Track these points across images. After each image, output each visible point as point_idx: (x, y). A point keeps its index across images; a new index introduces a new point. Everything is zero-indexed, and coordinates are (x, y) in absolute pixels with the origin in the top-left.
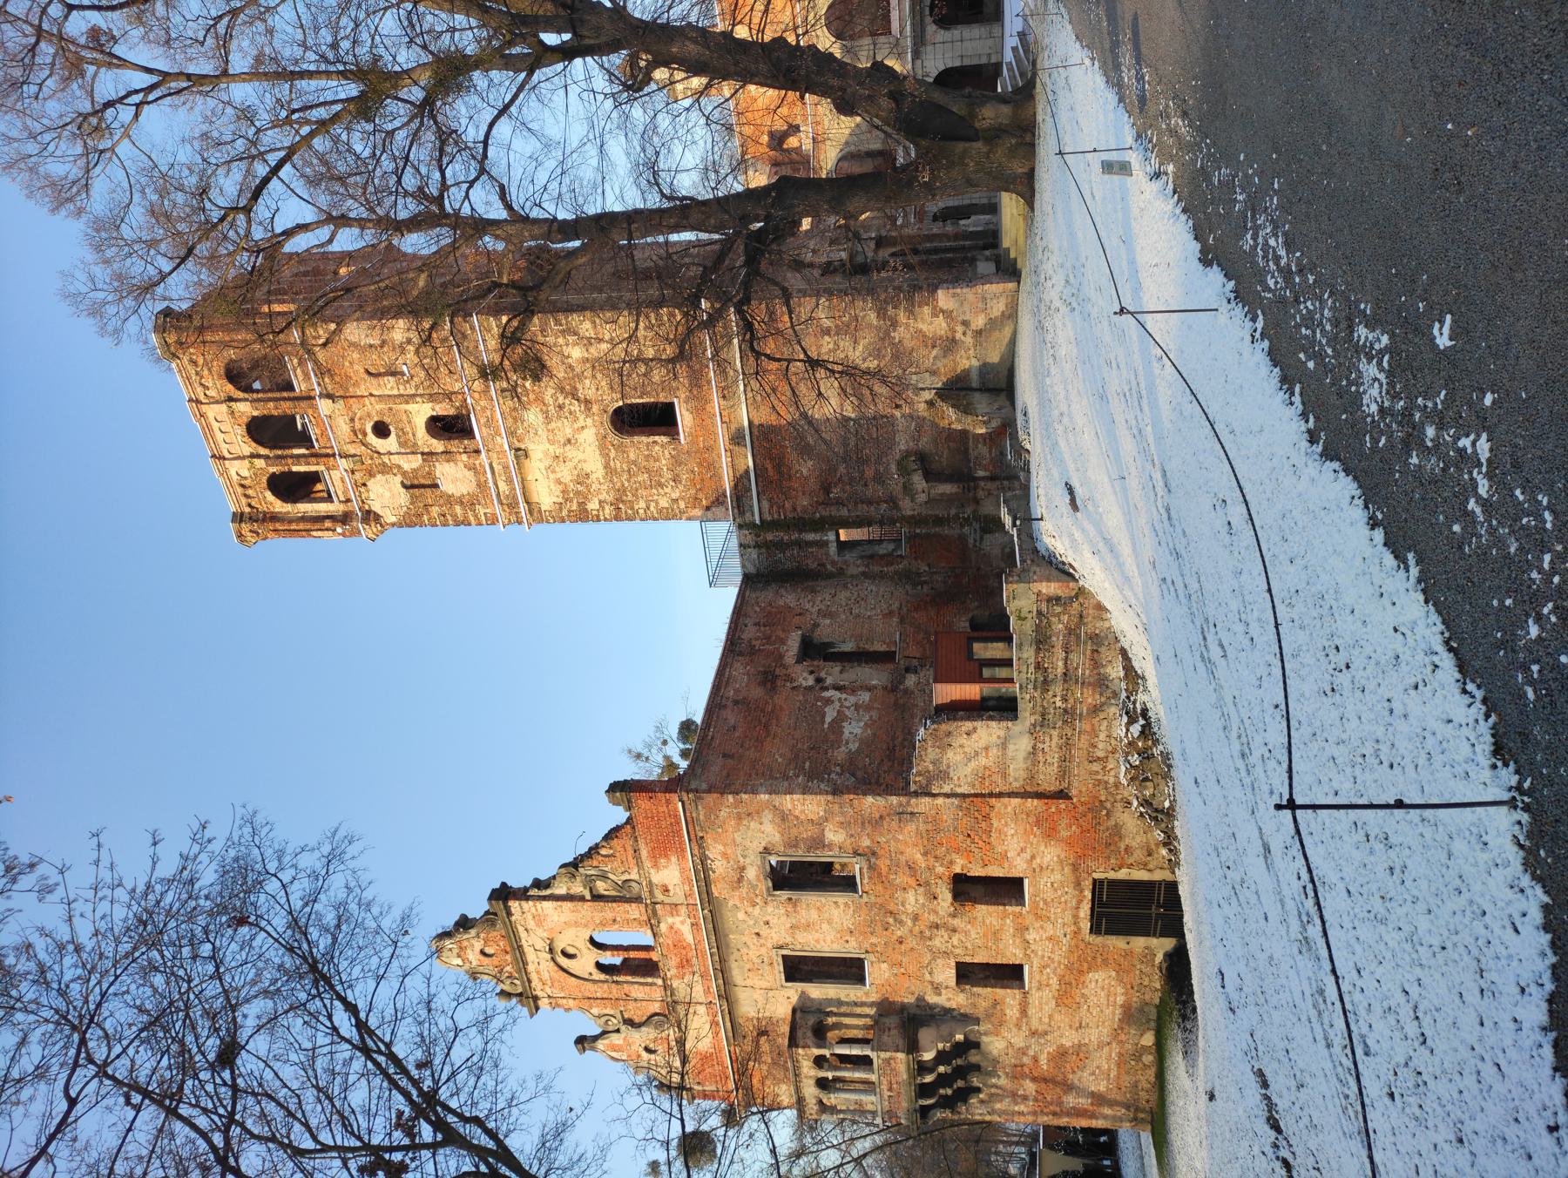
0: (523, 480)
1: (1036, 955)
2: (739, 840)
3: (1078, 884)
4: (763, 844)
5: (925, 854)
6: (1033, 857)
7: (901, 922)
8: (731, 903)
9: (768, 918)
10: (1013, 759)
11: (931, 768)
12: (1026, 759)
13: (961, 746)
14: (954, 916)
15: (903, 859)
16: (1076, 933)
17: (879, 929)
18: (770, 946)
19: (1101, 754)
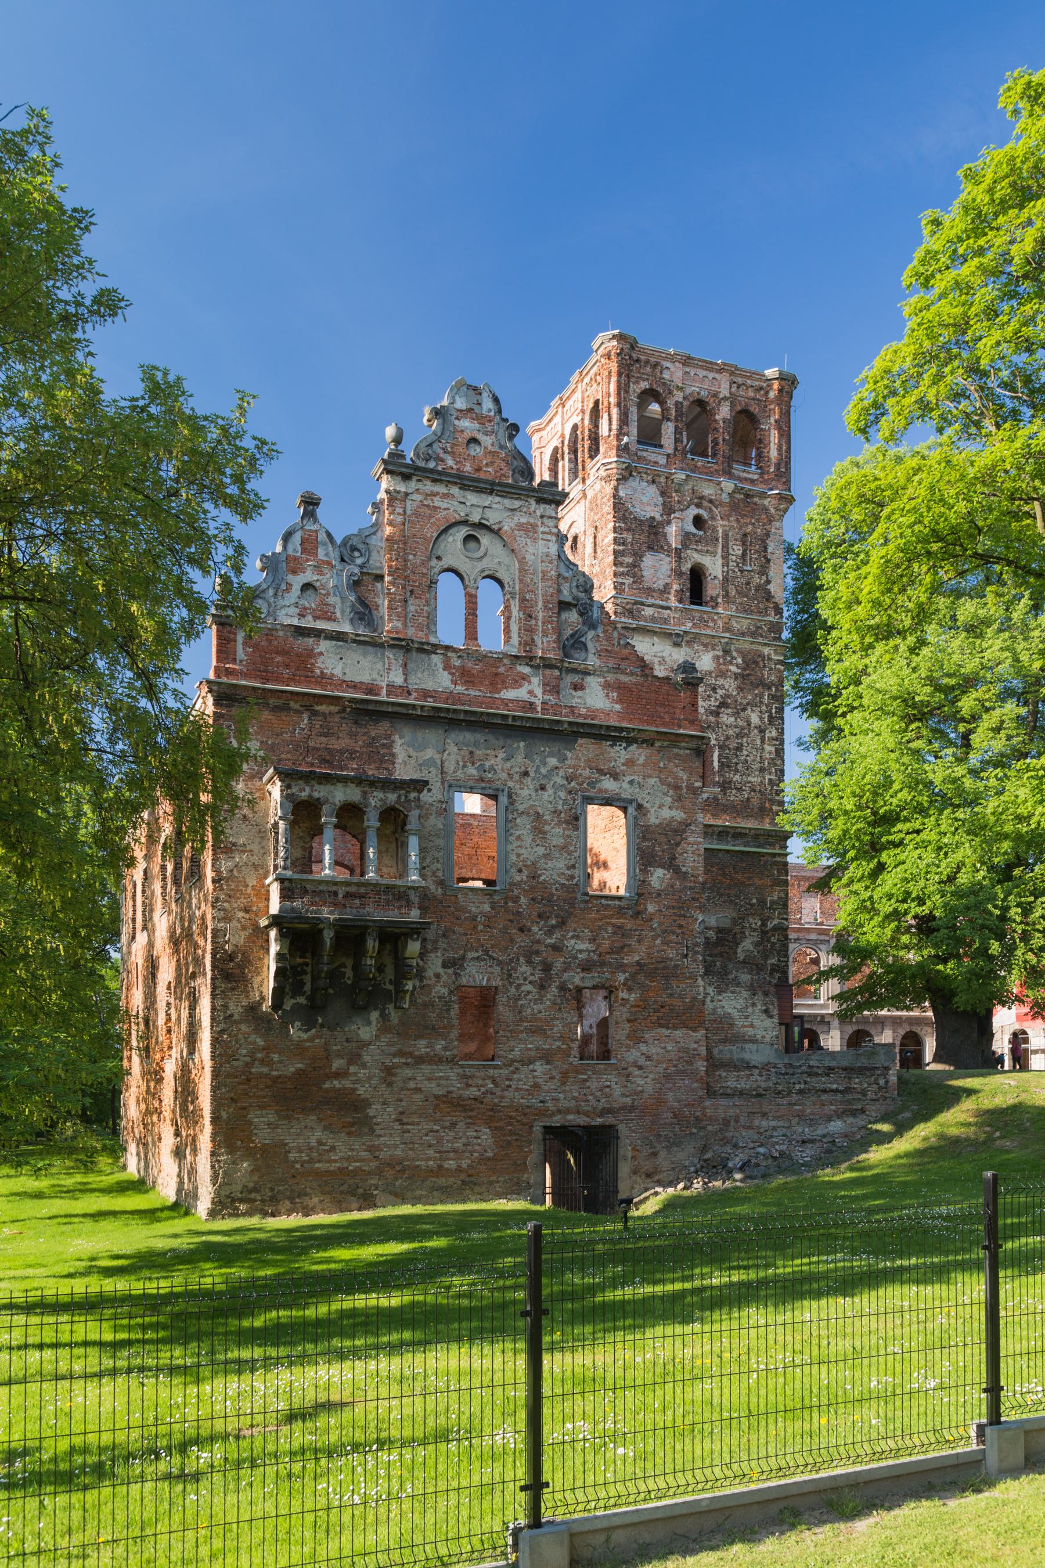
0: (655, 633)
1: (513, 1073)
2: (652, 781)
3: (605, 1112)
4: (645, 805)
5: (638, 963)
6: (640, 1068)
7: (550, 932)
8: (569, 755)
9: (550, 791)
10: (743, 1049)
11: (731, 977)
12: (742, 1060)
13: (754, 1005)
14: (563, 988)
15: (633, 942)
16: (543, 1113)
17: (538, 908)
18: (510, 784)
19: (756, 1123)
